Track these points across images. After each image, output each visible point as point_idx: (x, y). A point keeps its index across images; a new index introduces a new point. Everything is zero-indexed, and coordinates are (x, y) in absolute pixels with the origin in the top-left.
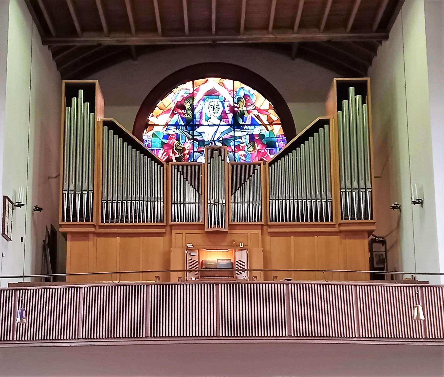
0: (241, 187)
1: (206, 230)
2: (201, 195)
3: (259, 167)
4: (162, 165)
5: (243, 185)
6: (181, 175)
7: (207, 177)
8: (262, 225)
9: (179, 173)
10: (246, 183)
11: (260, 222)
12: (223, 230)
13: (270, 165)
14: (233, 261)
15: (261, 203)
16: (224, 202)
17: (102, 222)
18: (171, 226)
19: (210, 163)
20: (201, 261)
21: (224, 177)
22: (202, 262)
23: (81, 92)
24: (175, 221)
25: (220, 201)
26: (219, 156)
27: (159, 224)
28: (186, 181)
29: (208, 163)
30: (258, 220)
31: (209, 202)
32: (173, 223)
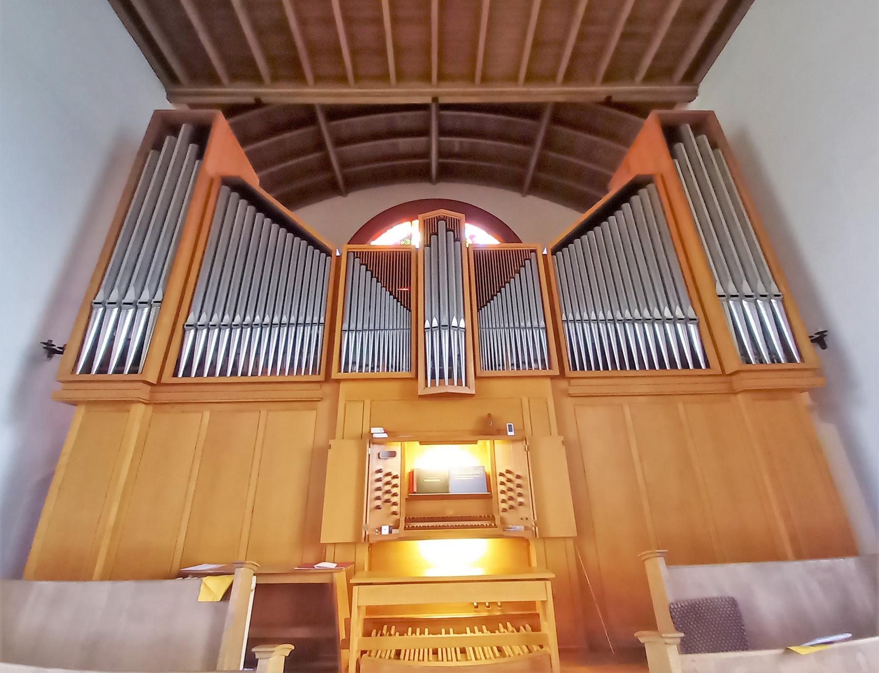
0: (499, 294)
1: (421, 391)
2: (410, 311)
3: (533, 254)
4: (329, 254)
5: (503, 289)
6: (367, 270)
7: (420, 273)
8: (552, 378)
9: (364, 267)
10: (507, 285)
11: (547, 372)
12: (463, 390)
13: (554, 252)
14: (488, 470)
15: (546, 328)
16: (462, 325)
17: (175, 374)
18: (338, 381)
19: (430, 246)
20: (408, 470)
21: (461, 283)
22: (412, 474)
23: (185, 130)
24: (346, 371)
25: (454, 323)
26: (447, 230)
27: (311, 377)
28: (377, 281)
29: (425, 246)
30: (544, 368)
31: (427, 325)
32: (342, 375)
